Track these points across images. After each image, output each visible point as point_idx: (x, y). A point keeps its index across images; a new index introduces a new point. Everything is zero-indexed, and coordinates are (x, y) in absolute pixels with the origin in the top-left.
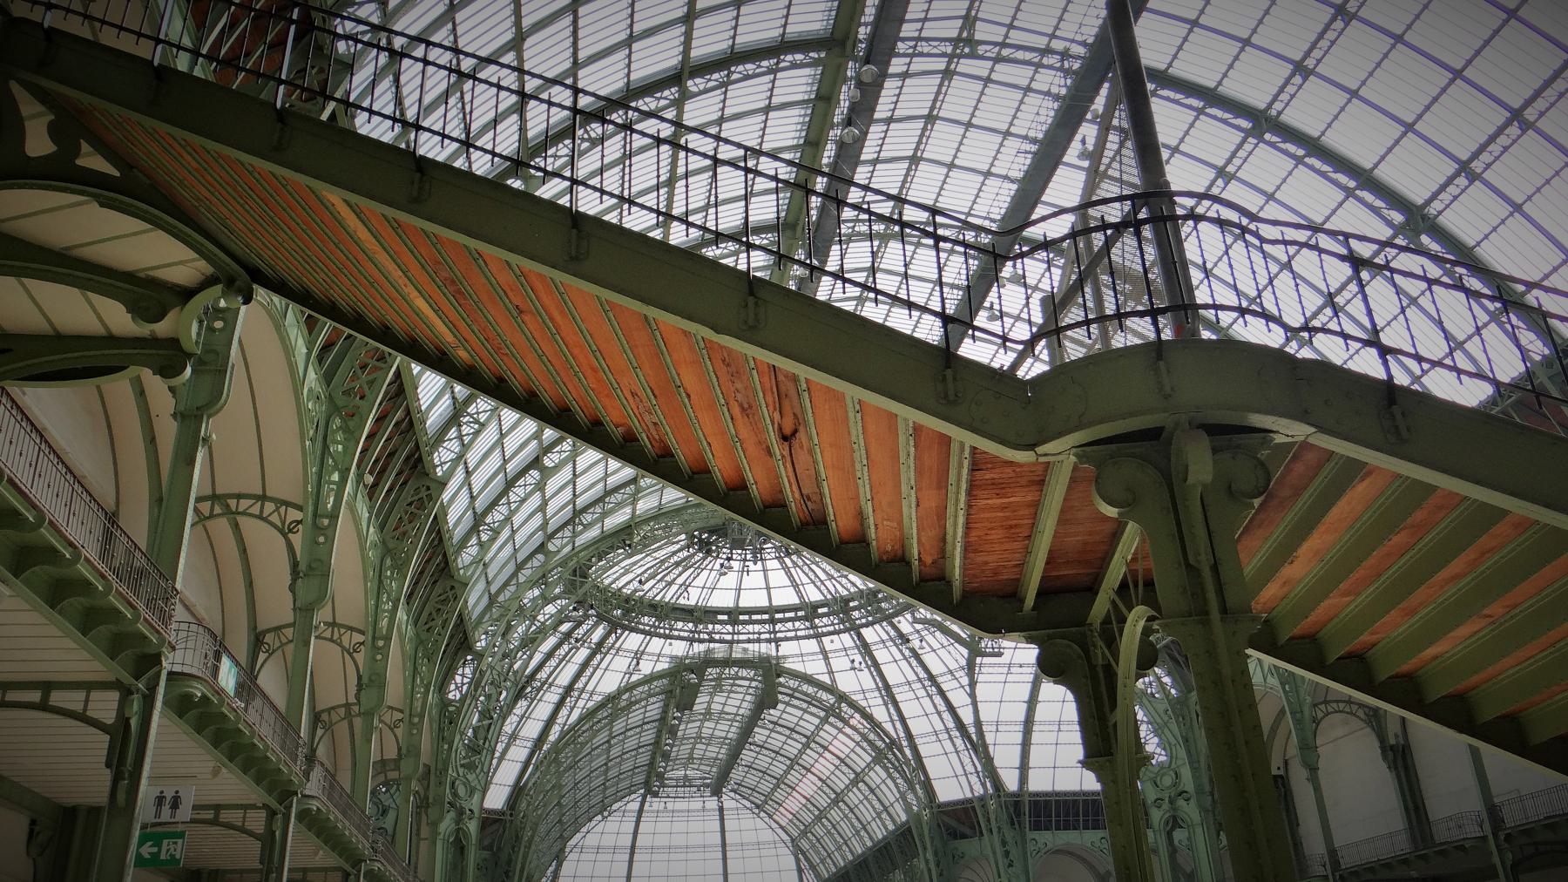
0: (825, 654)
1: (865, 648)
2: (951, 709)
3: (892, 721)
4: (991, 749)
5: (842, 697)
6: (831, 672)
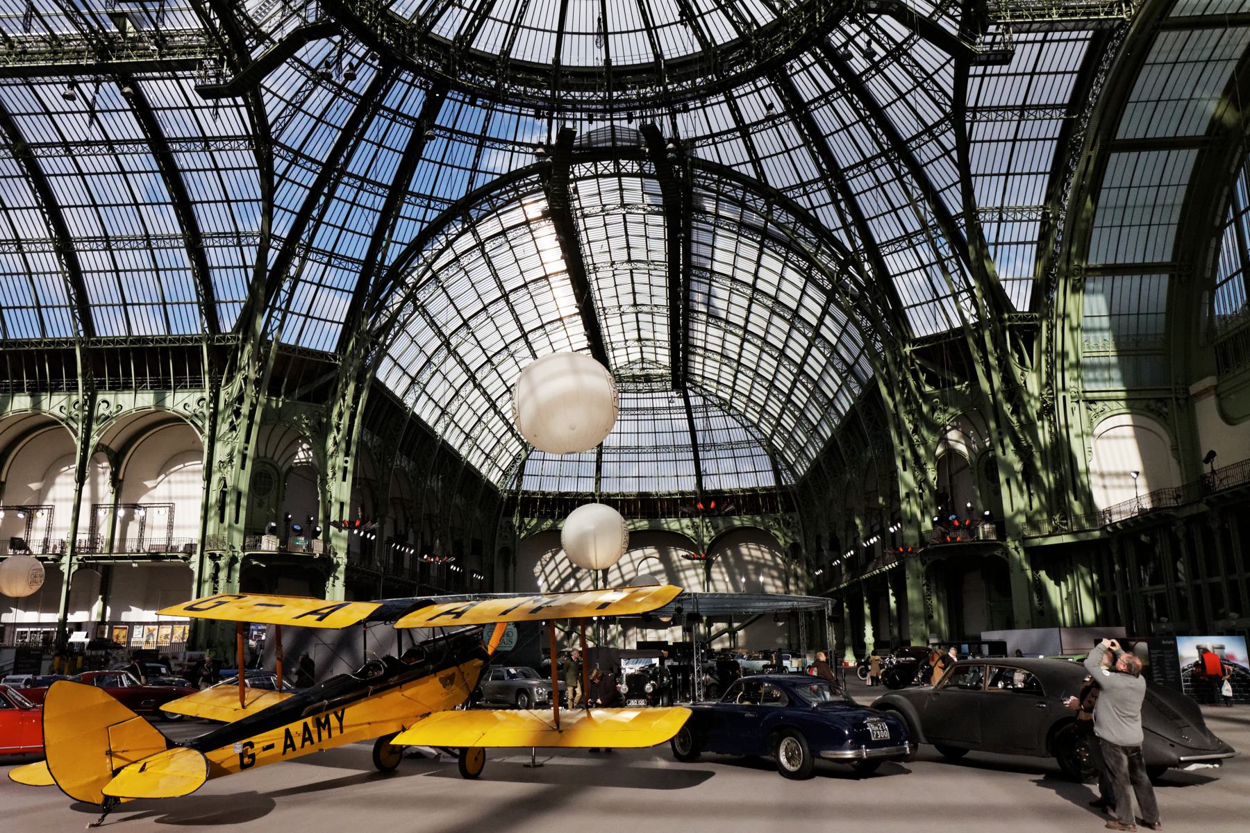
0: (743, 130)
1: (799, 111)
2: (931, 194)
3: (846, 227)
4: (991, 249)
5: (777, 198)
6: (756, 161)
